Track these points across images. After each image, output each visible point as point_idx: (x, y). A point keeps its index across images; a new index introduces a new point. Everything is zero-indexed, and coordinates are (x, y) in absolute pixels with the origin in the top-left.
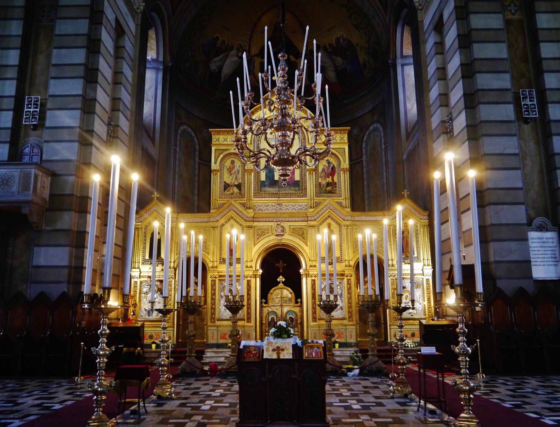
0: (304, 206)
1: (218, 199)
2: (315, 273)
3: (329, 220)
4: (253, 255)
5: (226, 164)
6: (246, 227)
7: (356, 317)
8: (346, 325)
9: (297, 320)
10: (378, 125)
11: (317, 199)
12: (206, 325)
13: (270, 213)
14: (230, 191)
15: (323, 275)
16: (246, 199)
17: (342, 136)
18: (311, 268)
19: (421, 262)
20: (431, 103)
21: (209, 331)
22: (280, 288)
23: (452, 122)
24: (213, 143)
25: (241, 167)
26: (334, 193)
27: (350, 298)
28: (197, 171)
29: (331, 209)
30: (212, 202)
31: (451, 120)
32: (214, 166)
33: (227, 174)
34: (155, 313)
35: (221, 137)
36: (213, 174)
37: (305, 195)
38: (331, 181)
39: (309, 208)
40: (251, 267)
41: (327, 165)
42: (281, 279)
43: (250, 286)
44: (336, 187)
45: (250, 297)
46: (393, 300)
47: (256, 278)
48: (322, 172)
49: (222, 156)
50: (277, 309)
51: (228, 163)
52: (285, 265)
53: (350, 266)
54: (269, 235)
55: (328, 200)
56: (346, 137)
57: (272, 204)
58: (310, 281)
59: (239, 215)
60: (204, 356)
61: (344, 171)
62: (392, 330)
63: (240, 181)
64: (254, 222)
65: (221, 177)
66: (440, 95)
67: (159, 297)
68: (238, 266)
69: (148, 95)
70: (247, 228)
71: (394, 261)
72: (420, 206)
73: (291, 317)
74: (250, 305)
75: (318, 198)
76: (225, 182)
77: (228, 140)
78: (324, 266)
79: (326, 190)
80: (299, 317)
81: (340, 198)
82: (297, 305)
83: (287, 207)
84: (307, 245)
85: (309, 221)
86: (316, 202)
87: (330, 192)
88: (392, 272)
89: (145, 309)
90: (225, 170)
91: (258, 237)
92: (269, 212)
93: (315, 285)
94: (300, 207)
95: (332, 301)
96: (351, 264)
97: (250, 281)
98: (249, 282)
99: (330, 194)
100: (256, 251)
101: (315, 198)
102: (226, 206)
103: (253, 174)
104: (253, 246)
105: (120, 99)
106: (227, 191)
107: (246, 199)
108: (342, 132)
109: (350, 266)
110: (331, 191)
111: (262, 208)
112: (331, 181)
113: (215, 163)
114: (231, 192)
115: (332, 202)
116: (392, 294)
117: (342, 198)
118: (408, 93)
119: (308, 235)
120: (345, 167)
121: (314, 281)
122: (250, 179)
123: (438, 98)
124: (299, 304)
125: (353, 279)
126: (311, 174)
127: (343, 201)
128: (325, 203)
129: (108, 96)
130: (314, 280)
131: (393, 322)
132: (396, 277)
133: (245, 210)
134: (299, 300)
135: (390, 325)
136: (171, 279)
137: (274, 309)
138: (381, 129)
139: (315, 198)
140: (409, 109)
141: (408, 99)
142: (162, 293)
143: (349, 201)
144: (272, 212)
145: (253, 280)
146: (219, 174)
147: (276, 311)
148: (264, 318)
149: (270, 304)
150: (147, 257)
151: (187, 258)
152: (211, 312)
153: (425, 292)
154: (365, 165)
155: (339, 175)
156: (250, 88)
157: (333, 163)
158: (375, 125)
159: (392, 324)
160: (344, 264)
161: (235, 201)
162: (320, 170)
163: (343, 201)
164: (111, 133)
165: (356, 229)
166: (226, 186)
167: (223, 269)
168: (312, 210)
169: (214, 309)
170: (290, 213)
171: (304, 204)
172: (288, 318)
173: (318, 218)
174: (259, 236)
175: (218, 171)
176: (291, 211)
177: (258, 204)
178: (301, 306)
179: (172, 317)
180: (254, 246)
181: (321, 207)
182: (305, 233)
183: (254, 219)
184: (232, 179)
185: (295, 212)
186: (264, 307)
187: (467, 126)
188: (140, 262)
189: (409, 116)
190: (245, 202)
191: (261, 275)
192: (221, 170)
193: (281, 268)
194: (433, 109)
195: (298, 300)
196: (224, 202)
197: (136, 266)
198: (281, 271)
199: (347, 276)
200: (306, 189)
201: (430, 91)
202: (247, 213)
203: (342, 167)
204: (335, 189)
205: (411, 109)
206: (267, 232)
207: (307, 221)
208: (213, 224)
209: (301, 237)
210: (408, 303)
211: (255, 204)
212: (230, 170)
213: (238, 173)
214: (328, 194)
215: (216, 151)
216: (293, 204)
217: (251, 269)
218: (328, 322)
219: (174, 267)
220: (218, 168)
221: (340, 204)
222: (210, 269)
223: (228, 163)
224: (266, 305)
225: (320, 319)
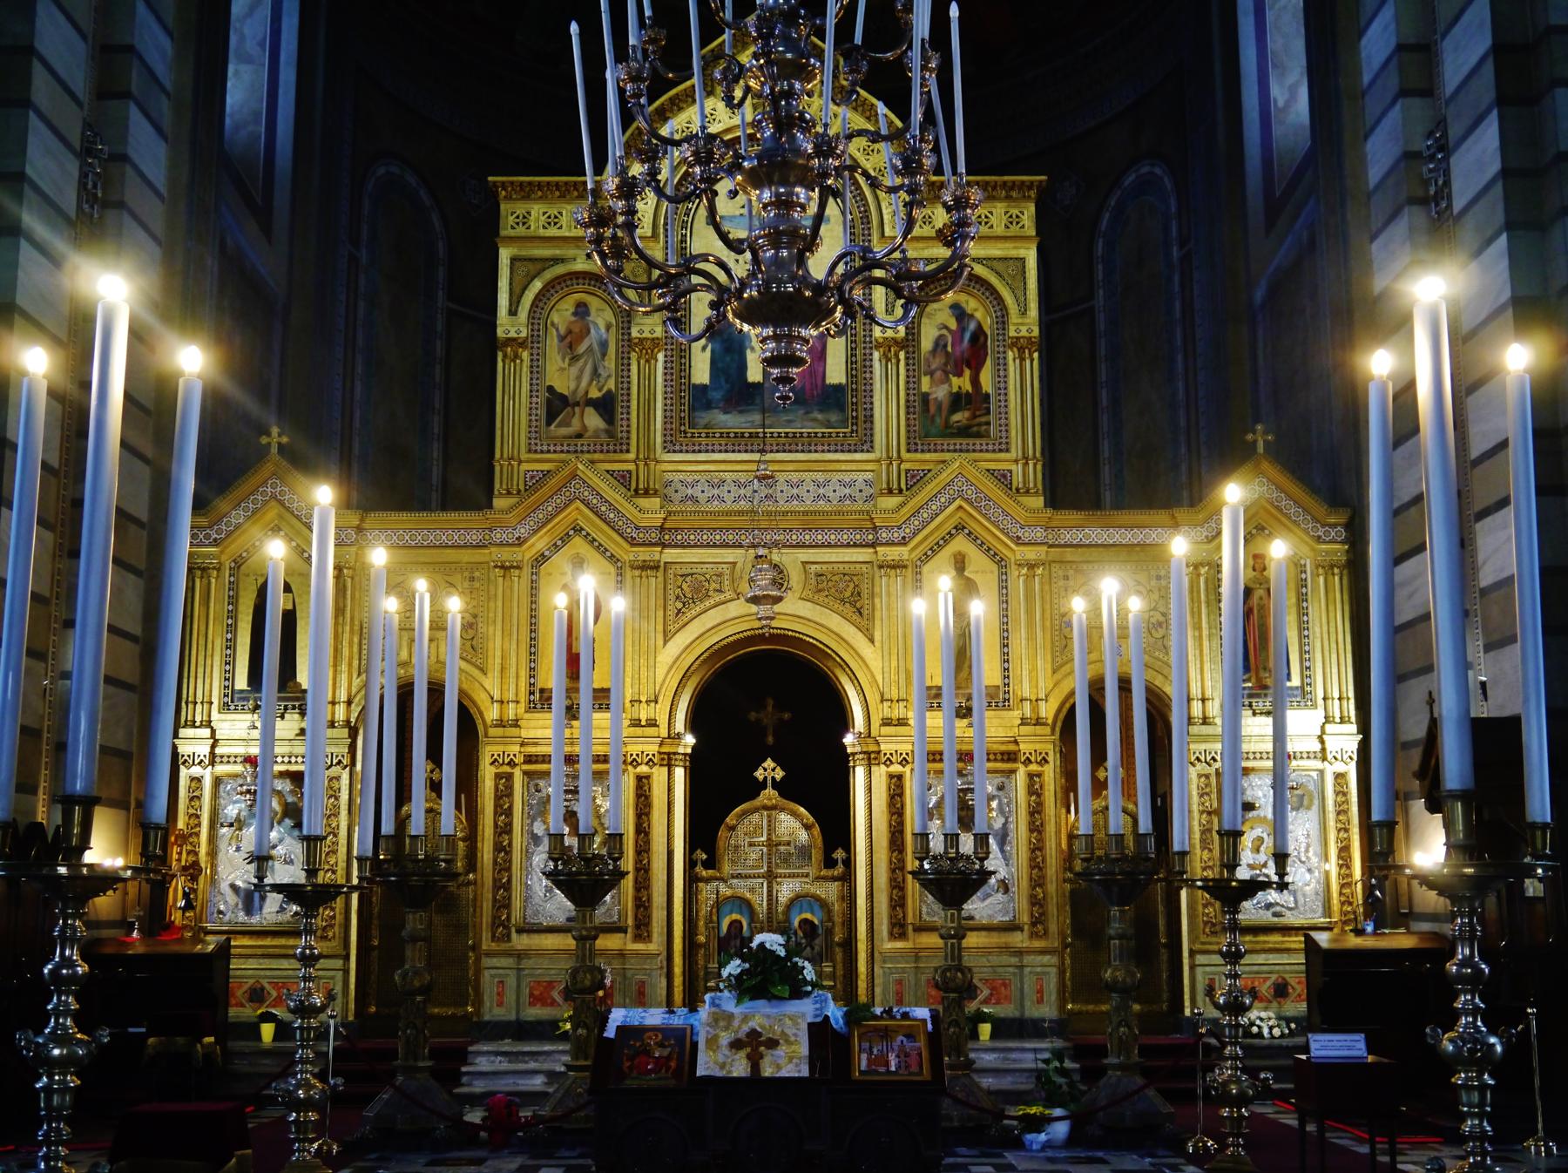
0: (860, 484)
1: (524, 456)
2: (905, 748)
3: (960, 544)
4: (659, 680)
5: (555, 317)
6: (633, 568)
7: (1059, 919)
8: (1020, 953)
9: (829, 932)
10: (1158, 171)
11: (913, 461)
12: (474, 948)
13: (728, 513)
14: (568, 425)
15: (935, 756)
16: (632, 456)
17: (1015, 212)
18: (886, 730)
19: (1315, 706)
20: (1366, 79)
21: (487, 973)
22: (766, 808)
23: (1446, 159)
24: (503, 233)
25: (613, 329)
26: (978, 435)
27: (1037, 848)
28: (438, 343)
29: (967, 500)
30: (497, 469)
31: (1441, 149)
32: (508, 325)
33: (559, 358)
34: (274, 900)
35: (537, 211)
36: (505, 356)
37: (866, 443)
38: (968, 387)
39: (882, 494)
40: (652, 723)
41: (953, 325)
42: (768, 770)
44: (988, 412)
45: (648, 842)
46: (1206, 855)
47: (669, 766)
48: (934, 351)
49: (537, 285)
50: (752, 890)
51: (562, 314)
52: (786, 716)
53: (1038, 722)
54: (723, 597)
55: (957, 462)
56: (1028, 213)
57: (734, 476)
59: (605, 521)
60: (464, 1069)
61: (1021, 350)
62: (1199, 970)
63: (611, 385)
64: (664, 546)
65: (537, 370)
66: (1400, 48)
67: (288, 840)
68: (601, 719)
69: (242, 38)
70: (637, 573)
71: (1209, 704)
72: (1314, 490)
73: (805, 922)
75: (919, 456)
76: (550, 389)
77: (564, 220)
78: (936, 721)
79: (947, 425)
80: (838, 919)
81: (1003, 455)
82: (830, 873)
83: (795, 491)
84: (872, 641)
85: (882, 544)
86: (907, 471)
87: (964, 432)
88: (1203, 747)
89: (234, 887)
90: (552, 342)
91: (679, 605)
92: (723, 507)
93: (901, 795)
94: (847, 491)
95: (968, 857)
96: (1043, 715)
97: (648, 777)
98: (642, 783)
99: (965, 441)
100: (670, 661)
101: (905, 455)
102: (553, 482)
103: (661, 356)
104: (660, 642)
105: (130, 49)
106: (559, 426)
107: (632, 456)
108: (1014, 194)
109: (1038, 722)
110: (968, 427)
111: (696, 492)
112: (968, 387)
113: (513, 312)
114: (576, 425)
115: (971, 473)
116: (1203, 833)
117: (1013, 455)
118: (1274, 43)
119: (877, 600)
120: (1024, 333)
121: (897, 782)
122: (651, 377)
123: (1395, 61)
124: (840, 869)
125: (1050, 773)
126: (888, 360)
127: (1013, 467)
128: (945, 477)
129: (84, 37)
130: (900, 777)
131: (1203, 938)
132: (1218, 765)
133: (629, 500)
134: (839, 854)
135: (1192, 953)
136: (335, 771)
137: (741, 888)
138: (1168, 183)
139: (905, 455)
140: (1281, 103)
141: (1275, 66)
142: (298, 825)
143: (1039, 467)
144: (736, 507)
145: (659, 775)
146: (525, 355)
147: (748, 895)
148: (701, 923)
149: (727, 869)
150: (241, 683)
151: (399, 688)
152: (495, 900)
153: (1331, 823)
154: (1101, 326)
155: (1001, 365)
156: (648, 13)
157: (978, 315)
158: (1145, 170)
159: (1197, 947)
160: (1017, 714)
161: (592, 462)
162: (927, 344)
163: (1013, 467)
164: (95, 186)
165: (1066, 578)
166: (557, 405)
167: (542, 729)
168: (891, 502)
169: (507, 887)
170: (806, 513)
171: (861, 477)
172: (796, 923)
173: (915, 534)
174: (686, 602)
175: (522, 344)
176: (808, 505)
177: (681, 476)
178: (848, 877)
179: (339, 918)
180: (665, 642)
181: (930, 489)
182: (865, 595)
183: (665, 536)
184: (579, 378)
185: (828, 508)
187: (1506, 173)
188: (215, 701)
189: (1277, 131)
190: (632, 467)
191: (690, 755)
192: (534, 341)
193: (770, 730)
194: (1372, 106)
195: (834, 856)
196: (546, 467)
197: (198, 719)
198: (770, 740)
199: (1028, 762)
200: (870, 419)
201: (1361, 33)
202: (635, 512)
203: (1012, 333)
204: (983, 419)
205: (1288, 104)
206: (714, 585)
207: (873, 545)
208: (506, 555)
209: (848, 609)
210: (1265, 865)
211: (669, 476)
212: (571, 341)
213: (604, 355)
214: (958, 441)
215: (518, 264)
216: (820, 477)
217: (651, 731)
218: (952, 937)
219: (348, 721)
220: (524, 334)
221: (1003, 478)
222: (492, 732)
223: (562, 314)
224: (711, 872)
225: (919, 929)
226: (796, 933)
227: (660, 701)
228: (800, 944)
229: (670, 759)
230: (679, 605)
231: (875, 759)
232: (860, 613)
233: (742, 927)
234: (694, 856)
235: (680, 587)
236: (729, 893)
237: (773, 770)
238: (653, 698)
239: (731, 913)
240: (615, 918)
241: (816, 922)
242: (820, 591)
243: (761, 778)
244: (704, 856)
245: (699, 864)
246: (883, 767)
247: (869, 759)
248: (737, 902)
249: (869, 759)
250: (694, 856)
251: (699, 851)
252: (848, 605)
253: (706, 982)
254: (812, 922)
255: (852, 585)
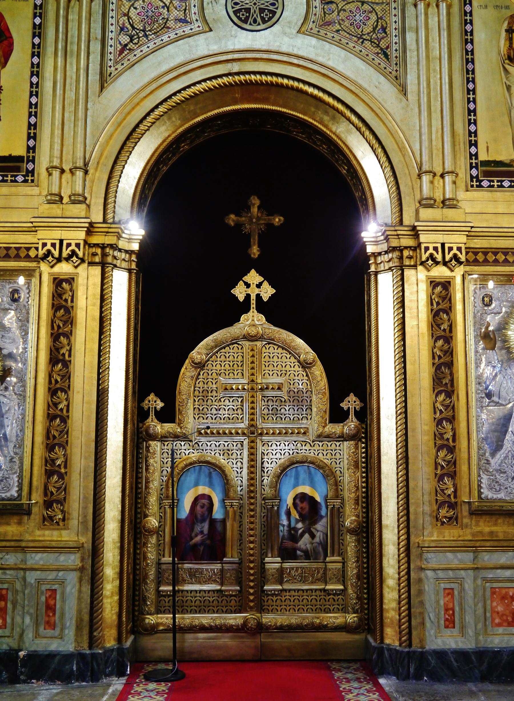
18: (425, 213)
22: (249, 338)
43: (68, 311)
45: (67, 376)
47: (103, 265)
50: (227, 453)
52: (277, 220)
58: (423, 287)
73: (303, 497)
74: (64, 420)
82: (336, 428)
84: (404, 91)
91: (125, 39)
93: (449, 310)
97: (71, 281)
119: (410, 37)
147: (222, 461)
148: (153, 500)
172: (289, 500)
186: (154, 437)
191: (140, 254)
195: (344, 405)
198: (255, 251)
206: (175, 13)
224: (168, 427)
226: (288, 513)
227: (91, 171)
228: (296, 529)
229: (104, 255)
230: (125, 39)
231: (410, 258)
232: (386, 56)
233: (211, 505)
234: (145, 405)
235: (127, 15)
236: (194, 456)
237: (259, 286)
238: (80, 163)
239: (196, 484)
240: (14, 492)
241: (318, 499)
242: (328, 24)
243: (241, 298)
244: (160, 405)
245: (152, 414)
246: (420, 268)
247: (401, 258)
248: (205, 470)
249: (401, 258)
250: (145, 405)
251: (152, 397)
252: (367, 44)
253: (159, 583)
254: (312, 500)
255: (374, 17)
